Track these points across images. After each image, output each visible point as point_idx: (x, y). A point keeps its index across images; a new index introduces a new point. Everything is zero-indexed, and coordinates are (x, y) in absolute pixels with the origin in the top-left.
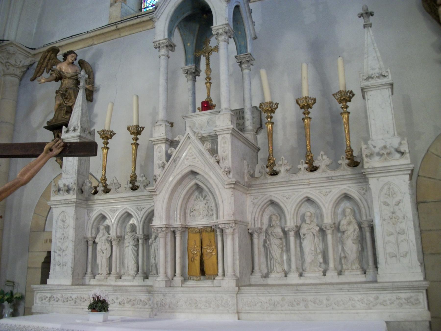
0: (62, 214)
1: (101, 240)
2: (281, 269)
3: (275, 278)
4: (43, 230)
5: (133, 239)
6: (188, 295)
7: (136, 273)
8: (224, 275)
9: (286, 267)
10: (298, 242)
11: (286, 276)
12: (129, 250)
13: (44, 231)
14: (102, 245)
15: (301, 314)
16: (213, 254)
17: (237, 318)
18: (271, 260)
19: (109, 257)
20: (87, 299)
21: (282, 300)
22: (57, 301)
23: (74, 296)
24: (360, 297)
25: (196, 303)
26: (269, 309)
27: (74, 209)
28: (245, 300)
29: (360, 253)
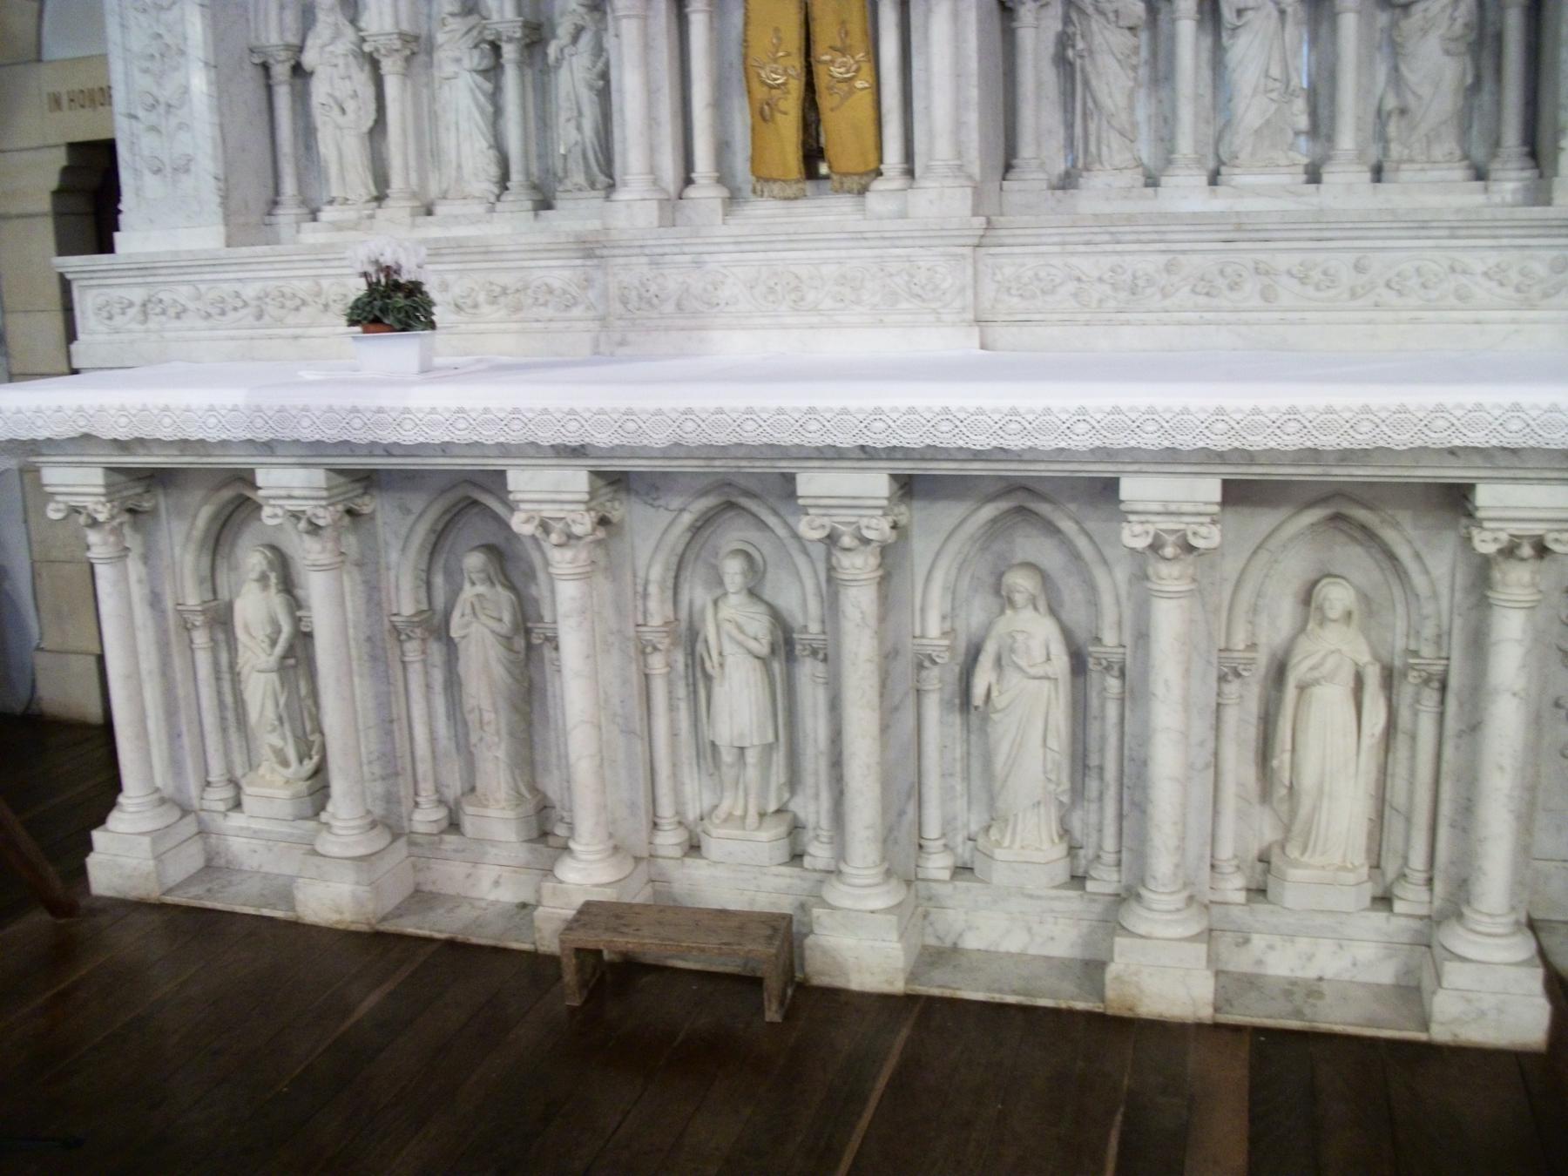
2: (1128, 155)
3: (1105, 190)
4: (33, 56)
5: (476, 46)
6: (761, 255)
7: (496, 190)
8: (910, 172)
9: (1146, 151)
10: (1207, 42)
11: (1152, 181)
12: (459, 90)
13: (39, 60)
14: (336, 82)
15: (1246, 323)
16: (859, 84)
17: (977, 343)
18: (1085, 116)
19: (371, 132)
20: (309, 299)
21: (1169, 268)
22: (178, 316)
23: (250, 291)
24: (1492, 259)
25: (796, 289)
26: (1112, 304)
28: (1008, 271)
29: (1466, 98)
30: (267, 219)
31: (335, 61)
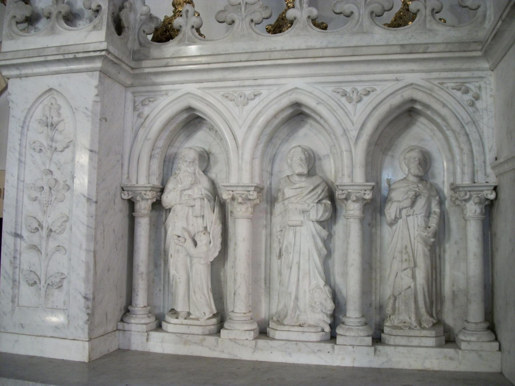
0: (47, 100)
1: (187, 198)
5: (319, 202)
27: (95, 82)
30: (121, 325)
31: (192, 203)
